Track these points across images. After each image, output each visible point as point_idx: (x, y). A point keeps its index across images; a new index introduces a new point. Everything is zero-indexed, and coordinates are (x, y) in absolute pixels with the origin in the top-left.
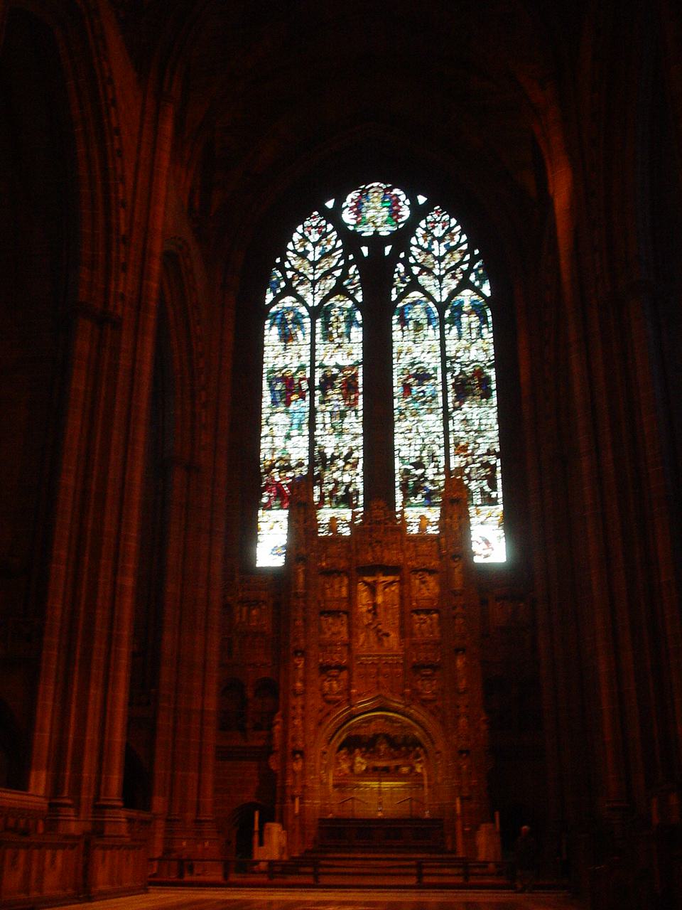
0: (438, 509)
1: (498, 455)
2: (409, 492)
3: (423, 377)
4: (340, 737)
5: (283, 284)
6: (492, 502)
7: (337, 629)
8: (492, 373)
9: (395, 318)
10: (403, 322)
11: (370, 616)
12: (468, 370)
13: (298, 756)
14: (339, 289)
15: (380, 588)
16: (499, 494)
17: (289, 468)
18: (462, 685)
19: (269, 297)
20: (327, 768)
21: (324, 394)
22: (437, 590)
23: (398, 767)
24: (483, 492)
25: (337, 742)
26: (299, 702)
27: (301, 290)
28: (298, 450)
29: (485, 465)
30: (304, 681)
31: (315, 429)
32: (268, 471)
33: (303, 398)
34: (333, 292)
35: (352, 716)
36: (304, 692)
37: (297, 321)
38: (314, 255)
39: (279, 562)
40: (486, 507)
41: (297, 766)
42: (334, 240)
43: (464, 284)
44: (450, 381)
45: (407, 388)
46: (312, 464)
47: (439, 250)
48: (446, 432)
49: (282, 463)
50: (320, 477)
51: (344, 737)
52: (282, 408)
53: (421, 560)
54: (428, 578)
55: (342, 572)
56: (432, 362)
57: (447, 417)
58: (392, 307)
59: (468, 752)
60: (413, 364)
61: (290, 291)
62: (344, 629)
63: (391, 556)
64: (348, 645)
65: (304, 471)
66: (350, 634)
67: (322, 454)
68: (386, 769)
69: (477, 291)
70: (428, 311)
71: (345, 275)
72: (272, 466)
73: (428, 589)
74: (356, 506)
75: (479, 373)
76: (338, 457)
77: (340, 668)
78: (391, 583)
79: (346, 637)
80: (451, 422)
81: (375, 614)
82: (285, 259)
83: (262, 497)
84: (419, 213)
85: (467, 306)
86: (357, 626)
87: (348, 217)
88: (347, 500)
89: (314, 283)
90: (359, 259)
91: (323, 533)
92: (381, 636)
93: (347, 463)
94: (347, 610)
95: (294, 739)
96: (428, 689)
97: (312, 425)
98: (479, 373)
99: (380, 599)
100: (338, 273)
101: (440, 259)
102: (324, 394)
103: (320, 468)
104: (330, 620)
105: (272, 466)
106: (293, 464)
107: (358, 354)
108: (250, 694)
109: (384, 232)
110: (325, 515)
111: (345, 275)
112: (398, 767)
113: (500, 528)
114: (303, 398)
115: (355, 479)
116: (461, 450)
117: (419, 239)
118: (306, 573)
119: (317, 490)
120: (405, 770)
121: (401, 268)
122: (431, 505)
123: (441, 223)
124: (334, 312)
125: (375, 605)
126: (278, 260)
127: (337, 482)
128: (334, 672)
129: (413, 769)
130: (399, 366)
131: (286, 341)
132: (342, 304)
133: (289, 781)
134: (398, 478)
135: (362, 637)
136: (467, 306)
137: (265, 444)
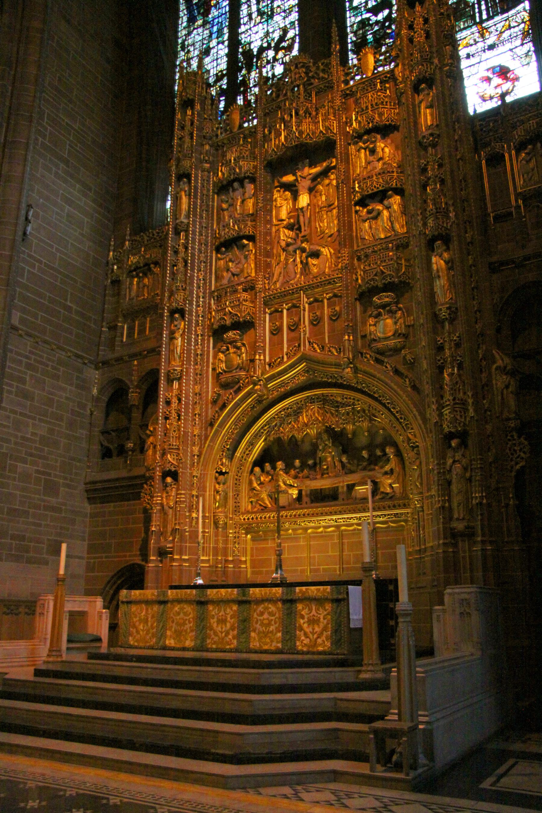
4: (252, 444)
13: (169, 480)
23: (351, 487)
31: (239, 25)
40: (497, 19)
51: (260, 445)
55: (245, 178)
67: (248, 54)
76: (269, 47)
93: (277, 49)
103: (244, 72)
113: (528, 39)
134: (351, 37)
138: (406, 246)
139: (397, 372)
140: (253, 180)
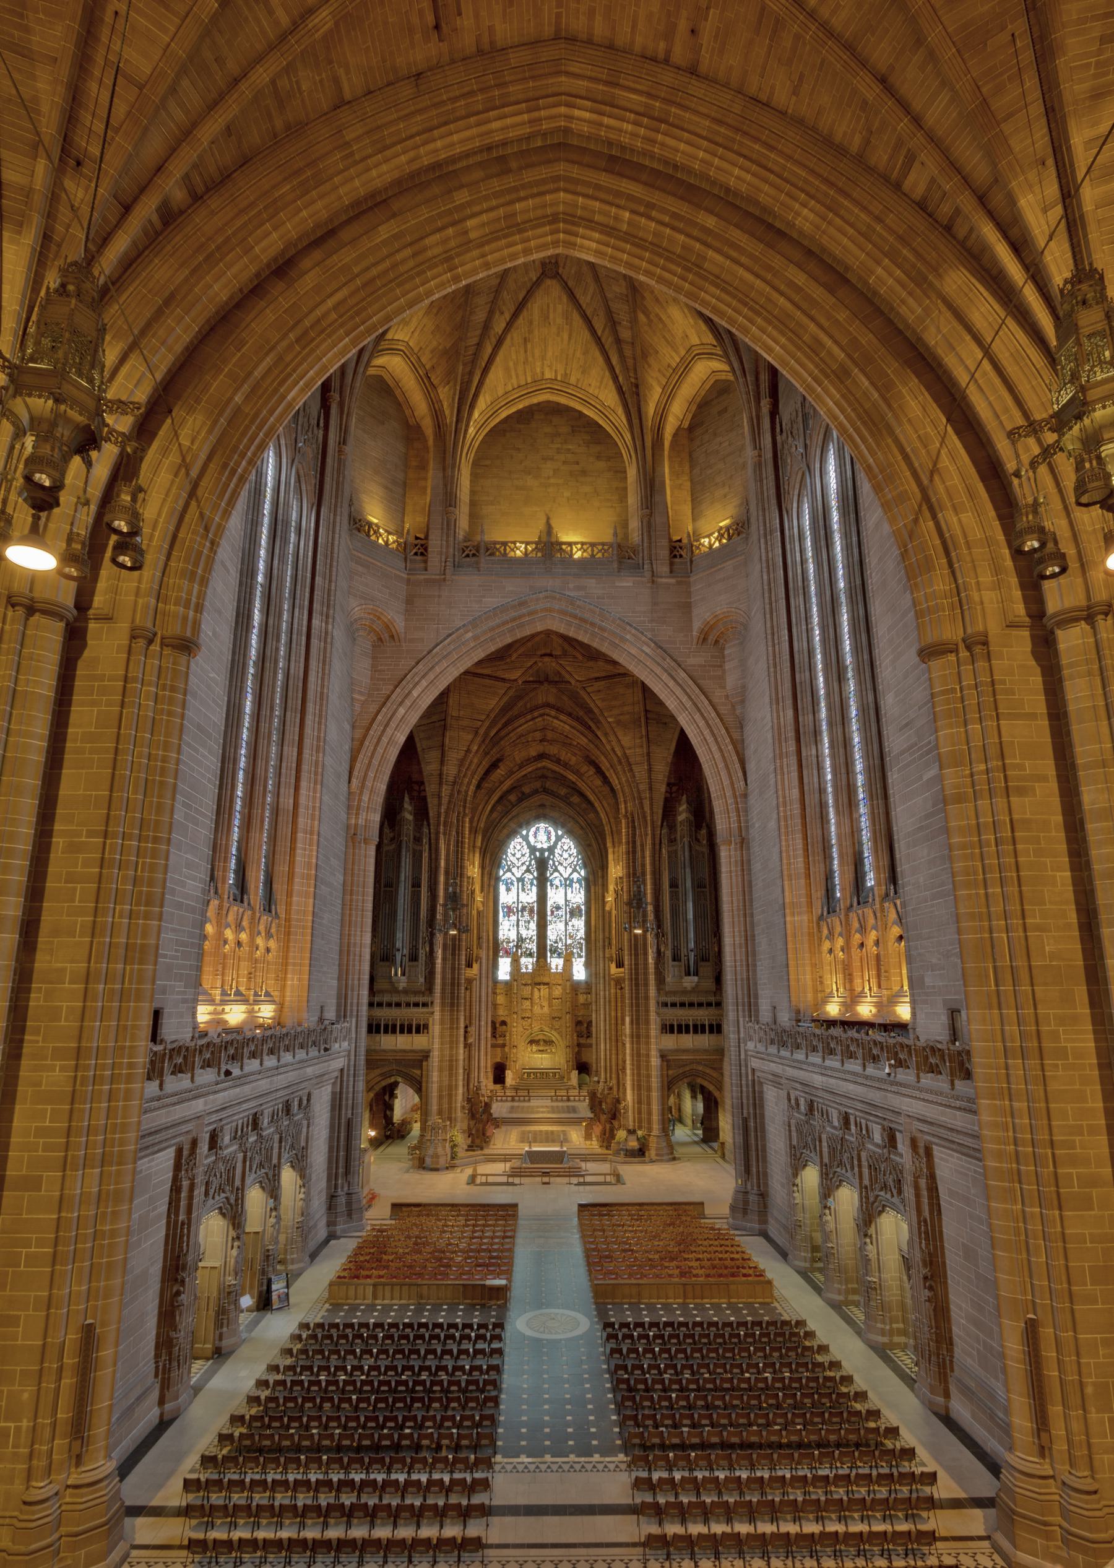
2: (554, 951)
3: (558, 908)
7: (528, 1003)
14: (528, 871)
28: (513, 936)
39: (508, 978)
42: (526, 851)
43: (575, 870)
47: (566, 855)
56: (562, 902)
58: (546, 879)
61: (509, 870)
63: (546, 980)
73: (557, 992)
75: (578, 907)
84: (558, 838)
87: (531, 839)
88: (531, 955)
92: (542, 1007)
96: (557, 1024)
109: (545, 846)
110: (523, 960)
115: (533, 947)
117: (557, 851)
123: (568, 843)
130: (550, 903)
132: (528, 876)
137: (501, 933)
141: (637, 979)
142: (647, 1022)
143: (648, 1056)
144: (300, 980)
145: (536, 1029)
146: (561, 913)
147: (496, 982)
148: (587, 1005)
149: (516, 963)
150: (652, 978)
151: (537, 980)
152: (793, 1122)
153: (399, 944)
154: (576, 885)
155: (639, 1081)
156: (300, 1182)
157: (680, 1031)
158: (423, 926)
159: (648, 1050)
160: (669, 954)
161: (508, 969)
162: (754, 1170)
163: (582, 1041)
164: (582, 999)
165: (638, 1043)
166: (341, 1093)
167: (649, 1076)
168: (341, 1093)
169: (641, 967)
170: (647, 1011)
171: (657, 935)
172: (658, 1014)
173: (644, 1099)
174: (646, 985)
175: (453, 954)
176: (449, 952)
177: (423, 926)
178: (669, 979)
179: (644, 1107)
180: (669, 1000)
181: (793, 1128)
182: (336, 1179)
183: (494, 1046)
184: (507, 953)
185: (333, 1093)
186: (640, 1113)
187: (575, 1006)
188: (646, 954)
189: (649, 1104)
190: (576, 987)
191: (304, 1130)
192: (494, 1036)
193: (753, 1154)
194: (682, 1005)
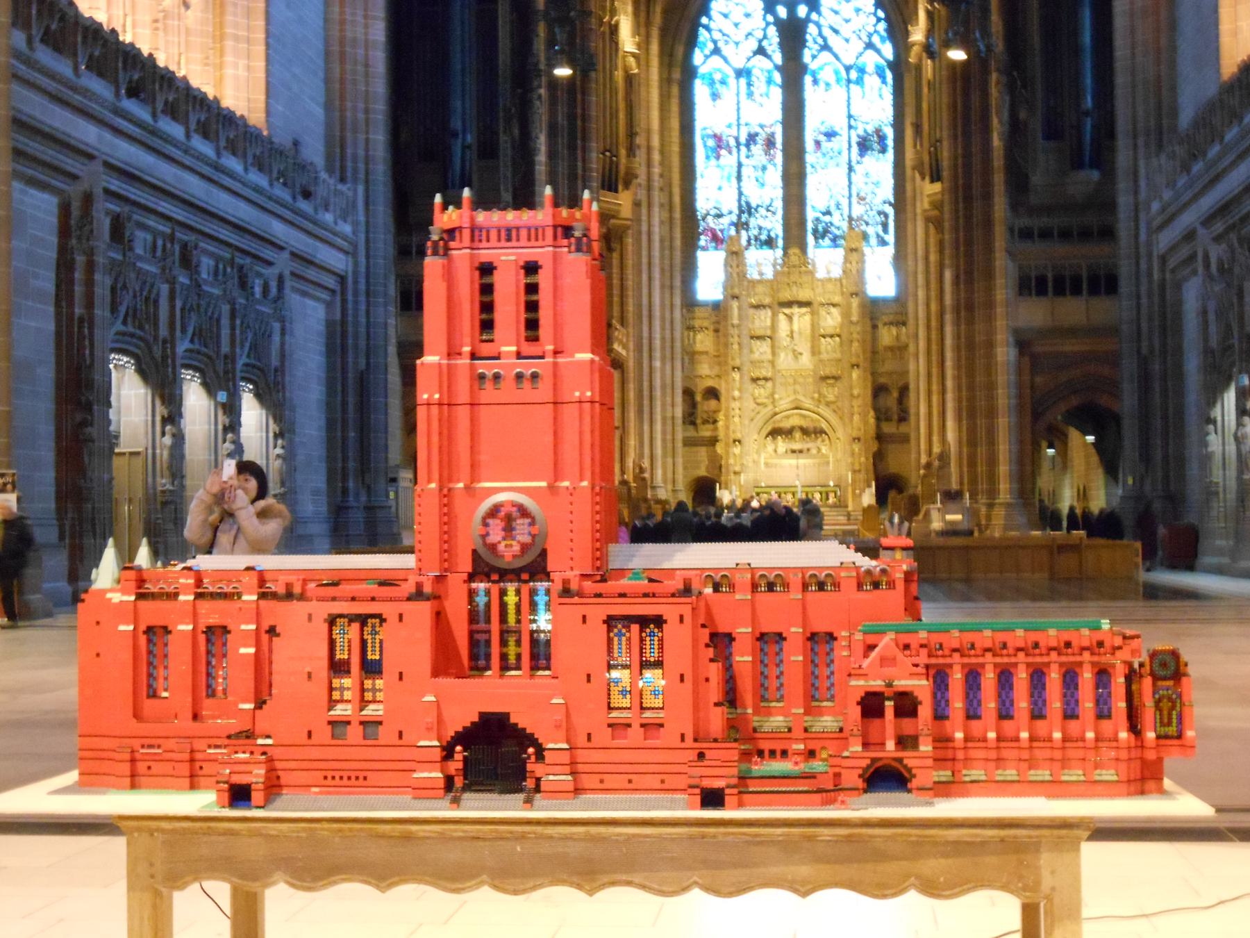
0: (840, 252)
1: (890, 204)
2: (819, 235)
3: (830, 135)
5: (711, 46)
6: (883, 243)
7: (763, 349)
8: (889, 133)
9: (808, 79)
10: (815, 82)
11: (788, 339)
12: (870, 129)
14: (761, 51)
15: (795, 319)
16: (890, 237)
17: (719, 216)
18: (856, 392)
19: (698, 57)
20: (758, 452)
21: (749, 150)
22: (839, 319)
23: (808, 450)
24: (878, 236)
25: (765, 432)
26: (735, 405)
27: (725, 50)
28: (729, 203)
29: (880, 213)
30: (740, 390)
32: (704, 219)
33: (730, 152)
34: (755, 53)
35: (776, 414)
36: (740, 398)
37: (723, 82)
38: (737, 15)
41: (737, 450)
44: (855, 140)
45: (818, 143)
46: (741, 212)
47: (847, 10)
48: (850, 183)
49: (713, 212)
50: (747, 224)
52: (713, 161)
53: (827, 296)
54: (833, 310)
57: (851, 169)
58: (803, 69)
59: (859, 439)
60: (823, 123)
62: (769, 350)
63: (804, 295)
64: (772, 363)
65: (734, 219)
66: (774, 354)
67: (748, 204)
68: (801, 451)
69: (878, 51)
70: (837, 73)
71: (765, 37)
72: (708, 214)
73: (831, 320)
74: (777, 247)
75: (878, 131)
77: (766, 379)
78: (804, 314)
79: (770, 357)
80: (853, 174)
81: (792, 337)
82: (710, 18)
83: (699, 239)
85: (870, 68)
86: (779, 348)
88: (770, 243)
89: (737, 44)
90: (778, 23)
91: (753, 274)
92: (797, 355)
94: (770, 337)
95: (734, 432)
96: (831, 393)
97: (739, 178)
98: (878, 131)
99: (796, 327)
100: (760, 35)
101: (847, 21)
102: (749, 150)
104: (758, 343)
105: (708, 214)
106: (725, 211)
107: (778, 114)
108: (698, 398)
111: (765, 37)
112: (808, 450)
114: (730, 152)
115: (775, 225)
116: (861, 199)
118: (740, 308)
119: (744, 233)
120: (814, 451)
121: (812, 29)
122: (836, 246)
124: (755, 72)
125: (792, 332)
126: (704, 20)
127: (760, 228)
128: (760, 383)
129: (819, 450)
131: (714, 100)
132: (760, 62)
133: (731, 461)
134: (810, 226)
135: (782, 355)
136: (870, 68)
138: (840, 360)
139: (835, 411)
140: (770, 307)
141: (968, 187)
142: (989, 275)
143: (990, 345)
144: (249, 68)
145: (784, 403)
146: (840, 143)
147: (690, 303)
148: (899, 350)
149: (735, 256)
150: (999, 179)
151: (786, 295)
152: (1212, 306)
153: (457, 124)
154: (872, 81)
155: (971, 400)
156: (273, 427)
157: (1060, 291)
158: (504, 85)
159: (990, 333)
160: (1036, 125)
161: (721, 276)
162: (1158, 455)
163: (888, 428)
164: (887, 336)
165: (970, 322)
166: (344, 322)
167: (991, 387)
168: (344, 322)
169: (976, 161)
170: (989, 249)
171: (1011, 88)
172: (1010, 253)
173: (982, 433)
174: (988, 196)
175: (572, 148)
176: (562, 141)
177: (504, 85)
178: (1037, 179)
179: (982, 451)
180: (1036, 223)
181: (1212, 317)
182: (345, 478)
183: (688, 443)
184: (716, 239)
185: (330, 324)
186: (972, 463)
187: (874, 353)
188: (986, 130)
189: (992, 442)
190: (873, 310)
191: (276, 338)
192: (690, 418)
193: (1158, 423)
194: (1065, 235)
